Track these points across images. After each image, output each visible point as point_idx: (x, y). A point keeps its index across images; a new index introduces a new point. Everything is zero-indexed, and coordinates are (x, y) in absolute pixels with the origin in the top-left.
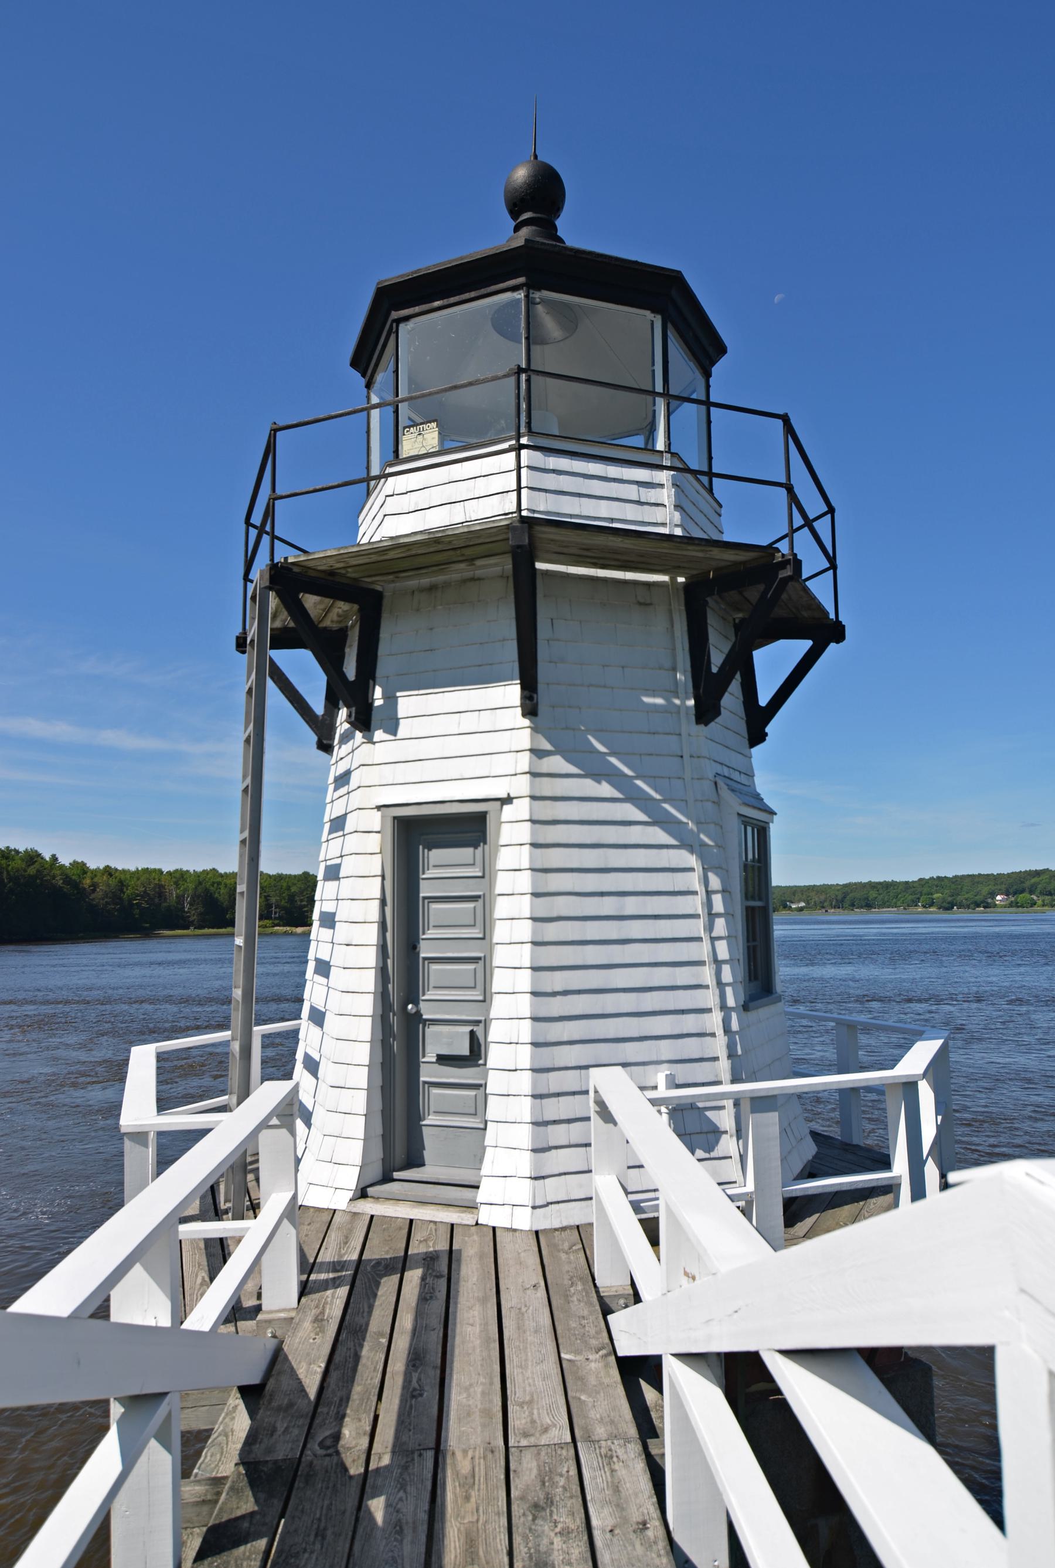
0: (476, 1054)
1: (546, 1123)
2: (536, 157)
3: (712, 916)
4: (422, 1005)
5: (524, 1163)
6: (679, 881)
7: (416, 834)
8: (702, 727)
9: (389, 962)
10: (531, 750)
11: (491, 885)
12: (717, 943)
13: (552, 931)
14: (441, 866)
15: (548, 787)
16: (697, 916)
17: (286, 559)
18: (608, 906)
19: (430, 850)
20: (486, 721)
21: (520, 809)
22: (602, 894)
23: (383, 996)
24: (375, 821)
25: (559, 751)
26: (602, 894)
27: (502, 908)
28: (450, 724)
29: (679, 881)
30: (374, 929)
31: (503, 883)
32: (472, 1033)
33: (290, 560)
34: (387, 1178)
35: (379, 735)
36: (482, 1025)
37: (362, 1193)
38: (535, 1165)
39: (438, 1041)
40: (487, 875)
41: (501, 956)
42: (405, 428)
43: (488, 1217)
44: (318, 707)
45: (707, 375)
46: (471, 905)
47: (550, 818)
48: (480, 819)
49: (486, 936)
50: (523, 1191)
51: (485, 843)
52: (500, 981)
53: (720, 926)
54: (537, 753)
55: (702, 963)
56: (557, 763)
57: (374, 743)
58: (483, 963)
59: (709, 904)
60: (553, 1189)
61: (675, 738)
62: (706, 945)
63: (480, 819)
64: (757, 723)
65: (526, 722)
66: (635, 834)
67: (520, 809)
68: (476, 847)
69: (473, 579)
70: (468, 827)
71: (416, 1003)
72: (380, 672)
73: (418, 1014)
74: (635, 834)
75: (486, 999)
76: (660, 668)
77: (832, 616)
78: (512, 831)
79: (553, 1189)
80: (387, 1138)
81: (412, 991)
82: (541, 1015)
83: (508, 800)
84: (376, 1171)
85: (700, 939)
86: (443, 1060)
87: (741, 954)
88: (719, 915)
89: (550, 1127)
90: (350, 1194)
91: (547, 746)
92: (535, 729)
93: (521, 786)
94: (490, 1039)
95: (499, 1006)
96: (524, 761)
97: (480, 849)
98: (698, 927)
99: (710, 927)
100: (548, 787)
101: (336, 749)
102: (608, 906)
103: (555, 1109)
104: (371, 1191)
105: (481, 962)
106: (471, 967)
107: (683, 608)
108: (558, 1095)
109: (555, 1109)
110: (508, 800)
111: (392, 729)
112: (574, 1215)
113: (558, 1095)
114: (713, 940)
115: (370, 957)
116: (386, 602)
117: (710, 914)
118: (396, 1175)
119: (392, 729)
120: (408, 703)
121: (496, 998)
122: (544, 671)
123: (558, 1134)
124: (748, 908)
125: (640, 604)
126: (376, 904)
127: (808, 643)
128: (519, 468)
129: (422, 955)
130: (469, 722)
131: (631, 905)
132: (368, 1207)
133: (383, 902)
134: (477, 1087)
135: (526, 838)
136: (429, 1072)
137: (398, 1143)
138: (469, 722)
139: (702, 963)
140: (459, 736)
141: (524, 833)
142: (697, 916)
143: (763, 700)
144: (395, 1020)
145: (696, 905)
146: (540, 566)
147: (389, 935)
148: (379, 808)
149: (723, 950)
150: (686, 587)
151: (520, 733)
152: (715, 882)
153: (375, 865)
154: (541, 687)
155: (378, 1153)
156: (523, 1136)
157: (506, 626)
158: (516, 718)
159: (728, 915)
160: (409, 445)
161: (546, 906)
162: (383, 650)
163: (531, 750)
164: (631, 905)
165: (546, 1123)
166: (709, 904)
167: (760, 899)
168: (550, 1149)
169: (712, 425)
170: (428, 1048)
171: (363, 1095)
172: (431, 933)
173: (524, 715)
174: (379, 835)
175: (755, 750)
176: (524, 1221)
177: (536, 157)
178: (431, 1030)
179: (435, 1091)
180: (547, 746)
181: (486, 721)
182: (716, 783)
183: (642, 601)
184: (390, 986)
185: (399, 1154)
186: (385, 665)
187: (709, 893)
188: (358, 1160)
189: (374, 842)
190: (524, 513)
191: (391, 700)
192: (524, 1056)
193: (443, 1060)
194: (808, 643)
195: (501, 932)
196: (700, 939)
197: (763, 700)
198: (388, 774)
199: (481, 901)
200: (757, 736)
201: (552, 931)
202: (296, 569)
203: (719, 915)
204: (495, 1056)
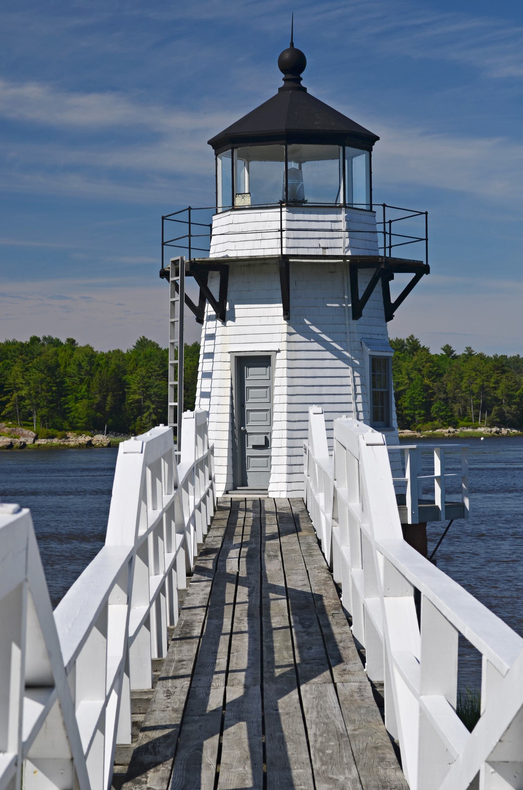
0: (267, 445)
1: (292, 465)
2: (292, 44)
3: (356, 394)
4: (246, 427)
5: (284, 478)
6: (344, 381)
7: (243, 363)
8: (355, 321)
9: (234, 411)
10: (287, 333)
11: (273, 383)
12: (358, 404)
13: (294, 399)
14: (253, 374)
15: (294, 346)
16: (350, 394)
17: (194, 259)
18: (316, 390)
19: (249, 368)
20: (270, 321)
21: (283, 355)
22: (313, 386)
23: (232, 424)
24: (228, 357)
25: (299, 332)
26: (313, 386)
27: (276, 391)
28: (256, 321)
29: (344, 381)
30: (229, 399)
31: (277, 382)
32: (266, 437)
33: (196, 260)
34: (235, 489)
35: (229, 323)
36: (269, 434)
37: (227, 492)
38: (288, 478)
39: (252, 440)
40: (271, 378)
41: (276, 408)
42: (237, 194)
43: (271, 495)
44: (196, 303)
45: (370, 150)
46: (265, 390)
47: (294, 358)
48: (269, 357)
49: (270, 402)
50: (284, 487)
51: (270, 366)
52: (276, 417)
53: (359, 398)
54: (289, 334)
55: (352, 412)
56: (298, 337)
57: (225, 326)
58: (269, 411)
59: (355, 390)
60: (294, 486)
61: (343, 326)
62: (353, 405)
63: (269, 357)
64: (390, 310)
65: (285, 322)
66: (327, 364)
67: (283, 355)
68: (267, 367)
69: (265, 264)
70: (264, 360)
71: (244, 426)
72: (228, 299)
73: (245, 431)
74: (327, 364)
75: (270, 425)
76: (338, 298)
77: (425, 263)
78: (280, 363)
79: (294, 486)
80: (234, 476)
81: (242, 422)
82: (290, 429)
83: (279, 351)
84: (231, 486)
85: (351, 403)
86: (255, 447)
87: (368, 408)
88: (359, 394)
89: (293, 466)
90: (223, 492)
91: (294, 331)
92: (289, 325)
93: (283, 346)
94: (272, 437)
95: (275, 426)
96: (285, 337)
97: (268, 368)
98: (351, 398)
99: (355, 398)
100: (294, 346)
101: (205, 322)
102: (316, 390)
103: (294, 460)
104: (229, 492)
105: (269, 411)
106: (265, 413)
107: (349, 272)
108: (296, 456)
109: (294, 460)
110: (279, 351)
111: (233, 319)
112: (302, 495)
113: (296, 456)
114: (356, 403)
115: (227, 409)
116: (230, 269)
117: (355, 394)
118: (238, 488)
119: (233, 319)
120: (240, 310)
121: (274, 423)
122: (293, 302)
123: (296, 469)
124: (373, 392)
125: (331, 272)
126: (229, 389)
127: (414, 275)
128: (281, 238)
129: (246, 409)
130: (264, 321)
131: (324, 390)
132: (229, 496)
133: (232, 389)
134: (267, 457)
135: (285, 366)
136: (249, 452)
137: (239, 477)
138: (264, 321)
139: (352, 412)
140: (259, 324)
141: (285, 363)
142: (350, 394)
143: (393, 300)
144: (236, 432)
145: (350, 390)
146: (290, 260)
147: (234, 401)
148: (229, 352)
149: (360, 407)
150: (350, 263)
151: (283, 326)
152: (358, 381)
153: (228, 374)
154: (291, 309)
155: (231, 481)
156: (284, 469)
157: (278, 285)
158: (281, 320)
159: (363, 394)
160: (239, 202)
161: (293, 390)
162: (229, 289)
163: (287, 333)
164: (324, 390)
165: (292, 465)
166: (355, 390)
167: (386, 388)
168: (293, 473)
169: (372, 174)
170: (250, 443)
171: (226, 459)
172: (250, 401)
173: (284, 320)
174: (229, 363)
175: (388, 323)
176: (284, 495)
177: (292, 44)
178: (250, 437)
179: (252, 459)
180: (294, 331)
181: (270, 321)
182: (361, 343)
183: (331, 270)
184: (235, 420)
185: (239, 481)
186: (231, 295)
187: (355, 386)
188: (225, 481)
189: (228, 366)
190: (284, 253)
191: (232, 309)
192: (284, 442)
193: (255, 447)
194: (414, 275)
195: (276, 400)
196: (351, 403)
197: (393, 300)
198: (232, 339)
199: (269, 388)
200: (389, 317)
201: (294, 399)
202: (198, 263)
203: (359, 394)
204: (274, 443)
